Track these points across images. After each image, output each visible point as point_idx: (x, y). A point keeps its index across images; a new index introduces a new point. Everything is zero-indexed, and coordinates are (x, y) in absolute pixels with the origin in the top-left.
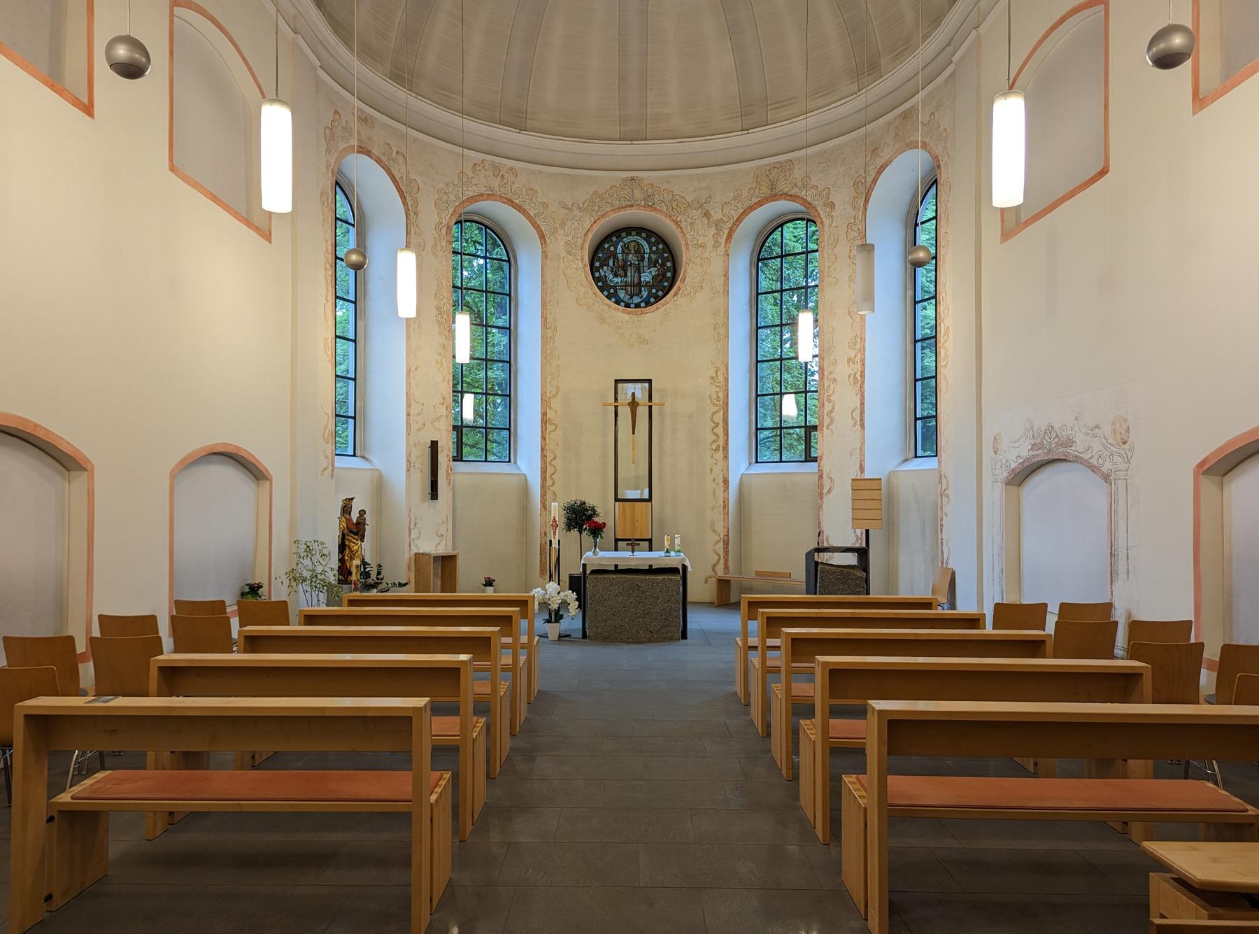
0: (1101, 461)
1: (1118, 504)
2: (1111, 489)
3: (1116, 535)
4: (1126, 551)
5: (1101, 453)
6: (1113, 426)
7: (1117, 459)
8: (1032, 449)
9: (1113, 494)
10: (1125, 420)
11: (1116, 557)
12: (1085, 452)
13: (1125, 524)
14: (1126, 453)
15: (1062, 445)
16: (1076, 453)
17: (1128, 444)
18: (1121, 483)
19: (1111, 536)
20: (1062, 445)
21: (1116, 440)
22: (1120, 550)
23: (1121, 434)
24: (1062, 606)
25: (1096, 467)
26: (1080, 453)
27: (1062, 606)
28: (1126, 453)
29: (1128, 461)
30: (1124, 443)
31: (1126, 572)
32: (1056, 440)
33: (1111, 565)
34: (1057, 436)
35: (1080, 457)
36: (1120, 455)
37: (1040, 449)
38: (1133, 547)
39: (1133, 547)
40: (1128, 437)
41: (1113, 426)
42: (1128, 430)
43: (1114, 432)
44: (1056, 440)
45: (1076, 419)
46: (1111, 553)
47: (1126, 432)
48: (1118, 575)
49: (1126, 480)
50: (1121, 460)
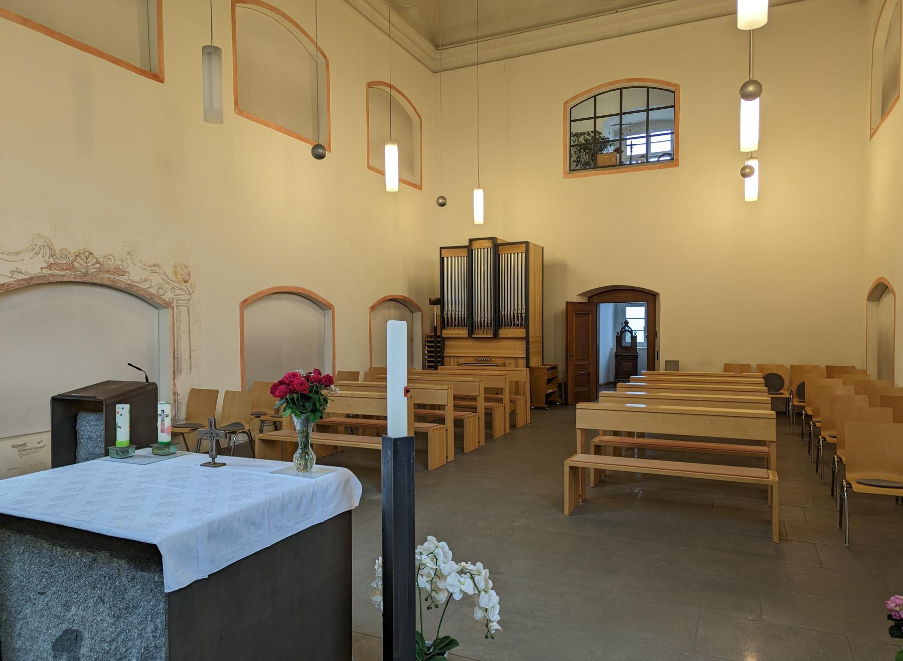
0: (161, 291)
1: (180, 322)
2: (174, 312)
3: (179, 344)
4: (189, 354)
5: (161, 285)
6: (174, 269)
7: (177, 292)
8: (50, 266)
9: (175, 316)
10: (187, 267)
11: (179, 359)
12: (142, 282)
13: (188, 336)
14: (188, 289)
15: (108, 272)
16: (129, 282)
17: (190, 283)
18: (184, 310)
19: (174, 345)
20: (108, 272)
21: (177, 278)
22: (183, 354)
23: (182, 275)
24: (227, 392)
25: (156, 296)
26: (136, 283)
27: (227, 392)
28: (188, 289)
29: (190, 294)
30: (186, 282)
31: (190, 367)
32: (98, 266)
33: (174, 365)
34: (98, 262)
35: (134, 286)
36: (182, 289)
37: (66, 270)
38: (195, 350)
39: (195, 350)
40: (190, 278)
41: (174, 269)
42: (189, 274)
43: (176, 273)
44: (98, 266)
45: (129, 253)
46: (174, 357)
47: (187, 274)
48: (181, 371)
49: (188, 307)
50: (182, 292)
